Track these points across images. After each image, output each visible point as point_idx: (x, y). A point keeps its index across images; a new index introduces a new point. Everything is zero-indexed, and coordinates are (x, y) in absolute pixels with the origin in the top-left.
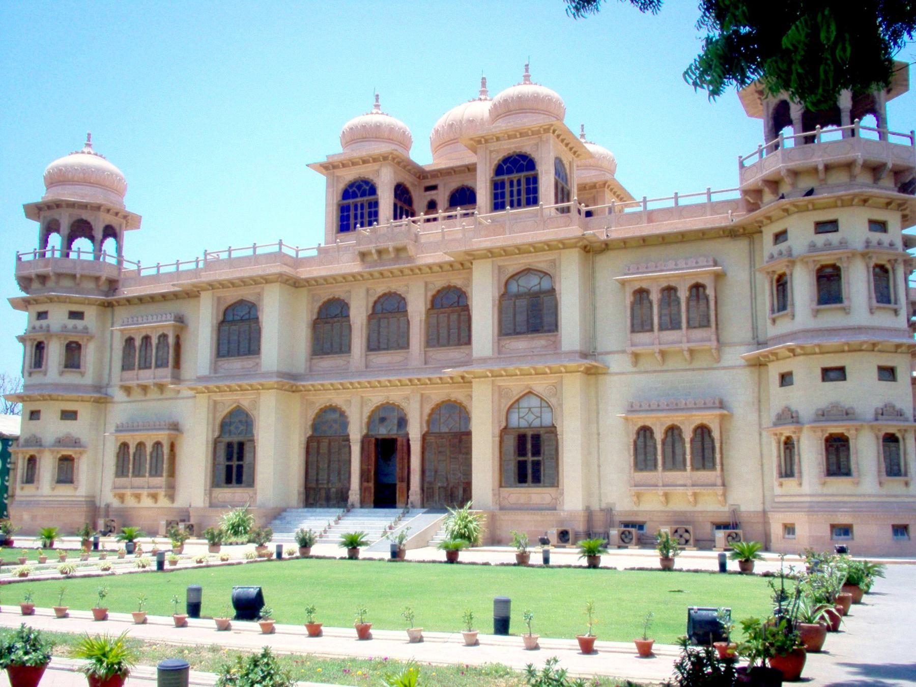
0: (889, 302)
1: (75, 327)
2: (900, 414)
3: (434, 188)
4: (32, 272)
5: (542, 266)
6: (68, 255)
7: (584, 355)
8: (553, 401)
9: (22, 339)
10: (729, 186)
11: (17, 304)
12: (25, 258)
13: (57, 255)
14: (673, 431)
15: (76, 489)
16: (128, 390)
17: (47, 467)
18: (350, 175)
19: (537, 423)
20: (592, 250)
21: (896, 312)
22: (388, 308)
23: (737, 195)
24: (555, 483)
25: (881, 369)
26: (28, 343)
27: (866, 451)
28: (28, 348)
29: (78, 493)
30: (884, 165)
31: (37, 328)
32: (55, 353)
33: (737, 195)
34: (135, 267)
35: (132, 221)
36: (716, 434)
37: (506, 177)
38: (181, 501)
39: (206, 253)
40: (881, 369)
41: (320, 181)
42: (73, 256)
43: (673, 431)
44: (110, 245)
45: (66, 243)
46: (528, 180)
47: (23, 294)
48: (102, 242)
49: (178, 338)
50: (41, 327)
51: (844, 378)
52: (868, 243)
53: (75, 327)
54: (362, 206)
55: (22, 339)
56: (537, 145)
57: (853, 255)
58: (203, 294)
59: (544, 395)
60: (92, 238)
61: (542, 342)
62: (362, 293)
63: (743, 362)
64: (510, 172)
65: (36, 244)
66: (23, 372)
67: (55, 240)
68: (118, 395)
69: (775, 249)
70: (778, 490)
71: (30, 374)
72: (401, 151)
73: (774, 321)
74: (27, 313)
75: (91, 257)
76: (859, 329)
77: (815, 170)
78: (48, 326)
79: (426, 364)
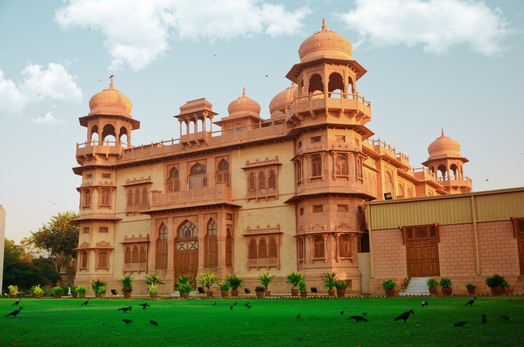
1: (106, 183)
4: (85, 153)
6: (102, 144)
11: (77, 171)
12: (80, 147)
13: (97, 144)
17: (93, 258)
26: (82, 192)
29: (109, 273)
42: (105, 144)
44: (124, 137)
45: (101, 137)
47: (80, 166)
48: (120, 136)
53: (106, 183)
55: (78, 189)
60: (114, 135)
65: (85, 139)
66: (80, 208)
75: (114, 145)
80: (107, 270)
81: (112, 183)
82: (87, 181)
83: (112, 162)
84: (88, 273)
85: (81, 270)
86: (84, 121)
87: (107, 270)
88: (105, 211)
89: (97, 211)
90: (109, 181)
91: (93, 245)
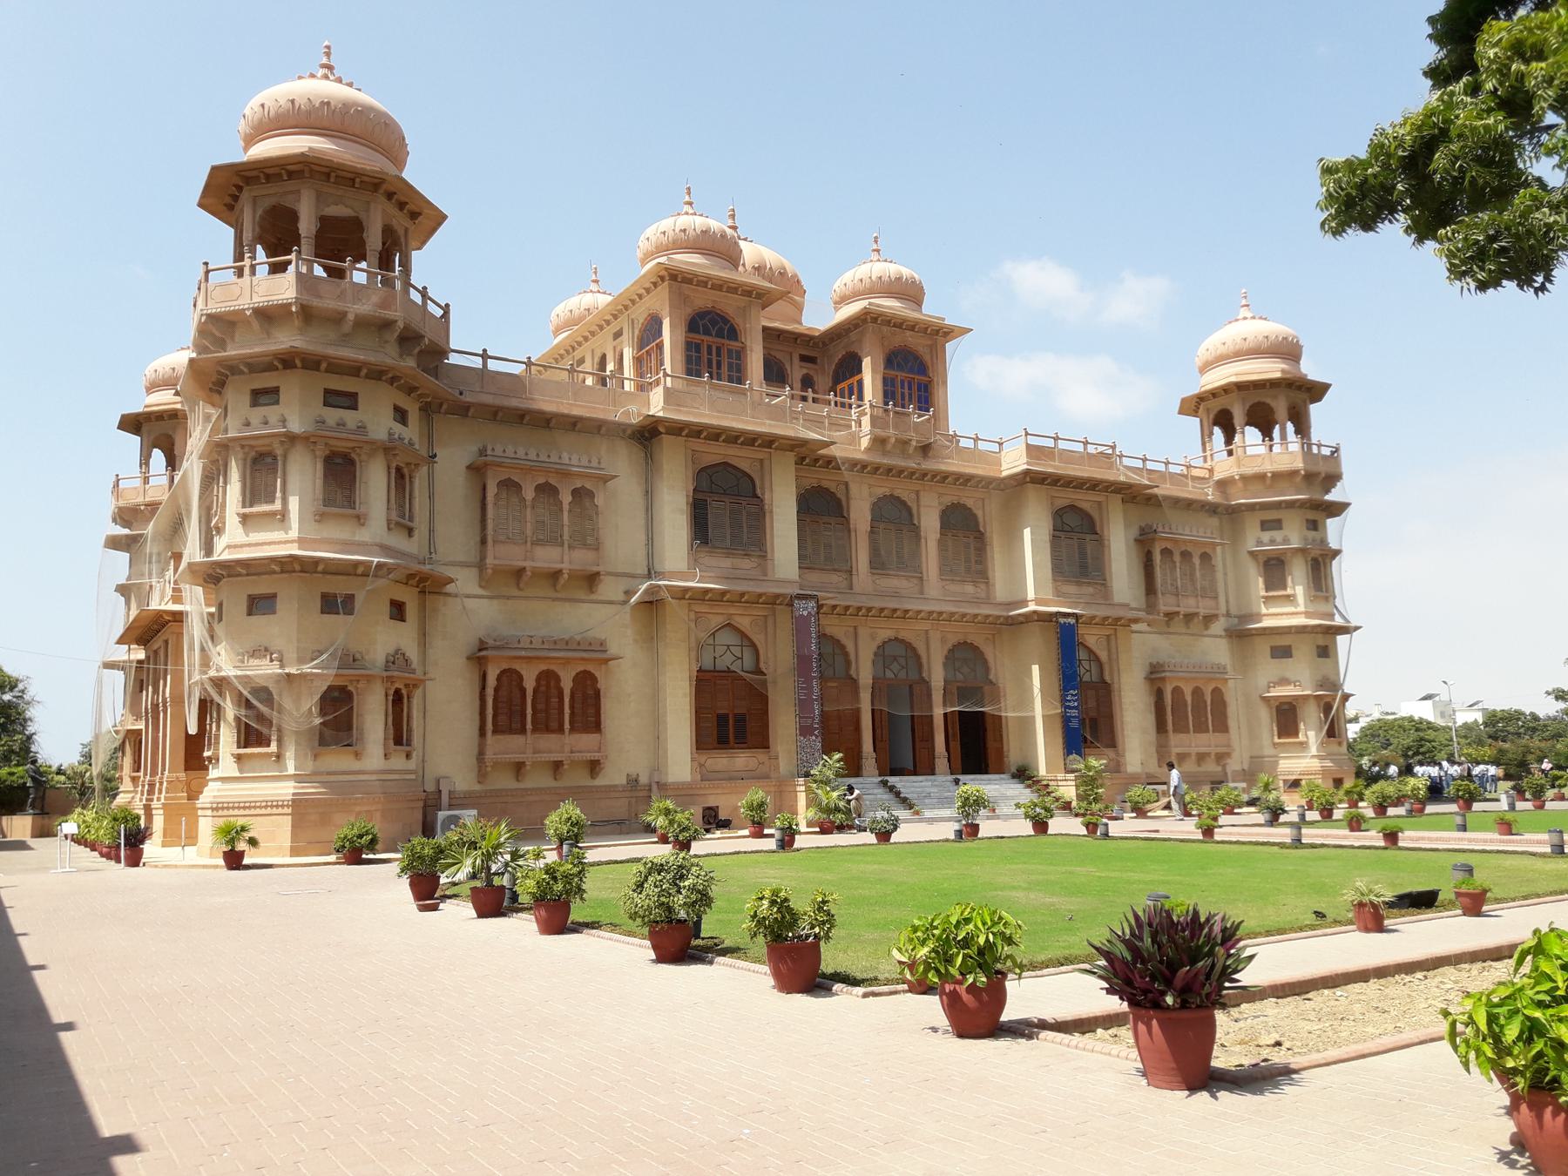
5: (1085, 506)
8: (1103, 656)
14: (1197, 692)
18: (703, 300)
19: (1086, 678)
22: (895, 516)
24: (1112, 743)
31: (331, 422)
32: (375, 483)
37: (901, 375)
43: (1197, 692)
46: (919, 385)
50: (341, 424)
54: (718, 349)
56: (931, 347)
58: (667, 440)
59: (1094, 648)
61: (1091, 590)
62: (865, 491)
64: (900, 368)
68: (465, 581)
69: (1266, 536)
71: (321, 517)
78: (362, 428)
82: (333, 415)
84: (356, 765)
87: (408, 756)
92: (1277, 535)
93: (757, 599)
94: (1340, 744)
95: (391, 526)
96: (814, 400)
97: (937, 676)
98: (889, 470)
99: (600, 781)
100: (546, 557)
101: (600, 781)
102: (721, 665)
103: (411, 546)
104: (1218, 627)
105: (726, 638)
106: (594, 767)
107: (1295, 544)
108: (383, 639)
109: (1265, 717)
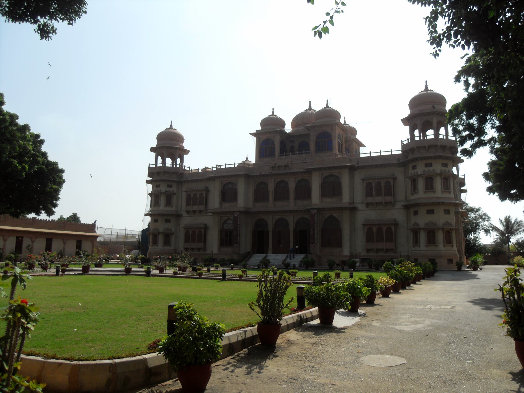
0: (448, 189)
2: (451, 224)
3: (294, 141)
5: (335, 174)
7: (350, 204)
9: (150, 194)
10: (397, 150)
11: (148, 182)
15: (170, 246)
16: (188, 212)
18: (264, 137)
20: (352, 169)
21: (450, 193)
23: (400, 152)
25: (445, 210)
27: (440, 236)
28: (153, 198)
30: (446, 146)
32: (163, 200)
33: (400, 152)
34: (188, 169)
35: (187, 152)
36: (393, 230)
38: (208, 251)
39: (217, 166)
40: (445, 210)
41: (255, 138)
49: (206, 195)
51: (433, 213)
52: (441, 170)
57: (437, 174)
63: (402, 207)
67: (160, 160)
68: (185, 214)
69: (413, 171)
70: (413, 249)
71: (154, 206)
72: (282, 129)
73: (412, 194)
74: (151, 185)
76: (438, 198)
77: (425, 147)
79: (295, 205)
80: (170, 246)
81: (173, 191)
82: (157, 189)
83: (174, 178)
85: (152, 246)
86: (153, 150)
88: (168, 209)
89: (162, 207)
90: (171, 189)
91: (161, 231)
92: (415, 171)
93: (230, 212)
94: (452, 246)
95: (166, 206)
96: (286, 155)
97: (291, 228)
98: (276, 174)
99: (206, 253)
100: (195, 208)
101: (206, 253)
102: (227, 228)
103: (174, 209)
104: (399, 205)
105: (230, 222)
106: (205, 249)
107: (419, 173)
108: (162, 227)
109: (411, 235)
